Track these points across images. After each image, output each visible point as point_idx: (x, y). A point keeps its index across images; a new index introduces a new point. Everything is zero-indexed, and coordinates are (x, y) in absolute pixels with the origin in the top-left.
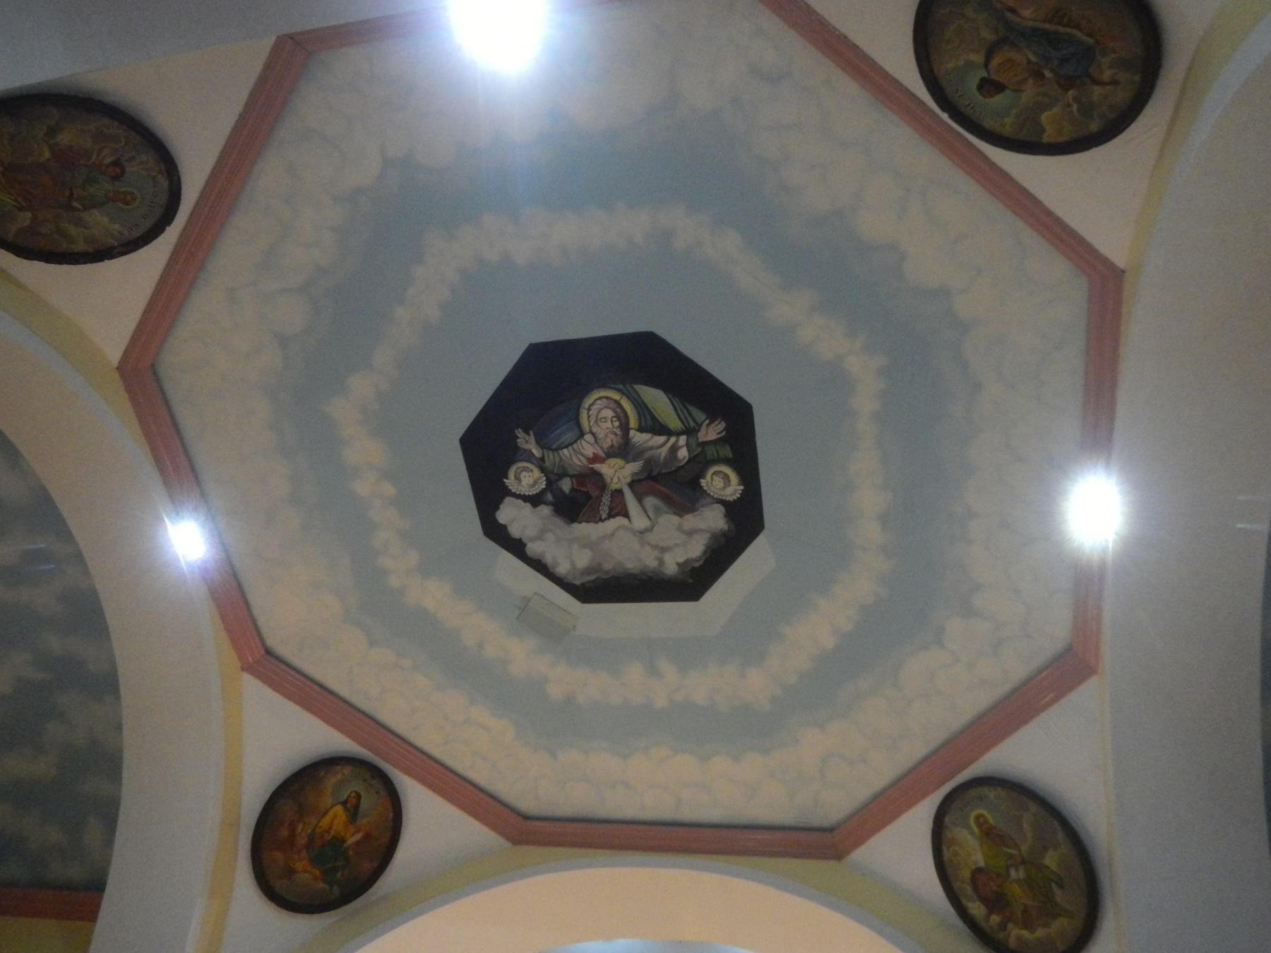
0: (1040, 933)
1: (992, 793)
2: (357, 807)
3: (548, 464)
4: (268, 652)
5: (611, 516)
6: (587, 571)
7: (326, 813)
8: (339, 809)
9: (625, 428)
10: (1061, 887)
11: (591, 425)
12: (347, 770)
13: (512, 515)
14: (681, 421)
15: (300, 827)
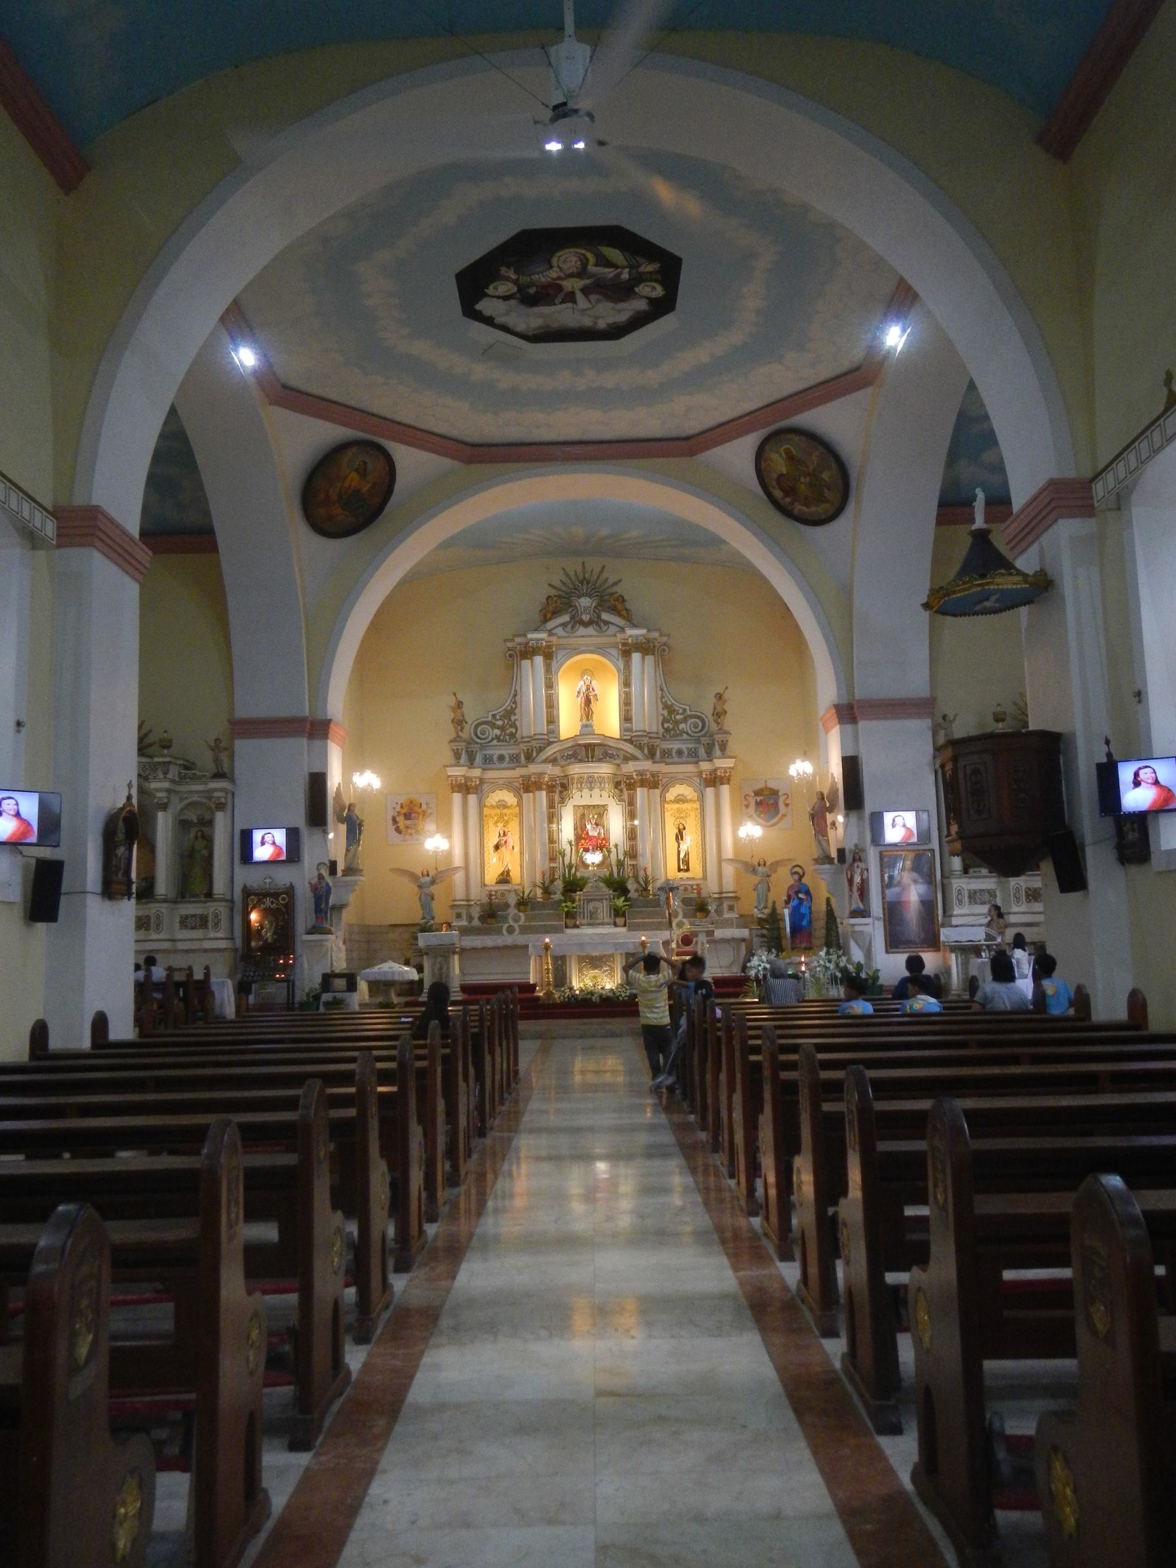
0: (813, 509)
1: (796, 438)
2: (365, 470)
3: (521, 281)
4: (284, 387)
5: (563, 302)
6: (539, 328)
7: (346, 478)
8: (354, 475)
9: (585, 263)
10: (829, 489)
11: (560, 262)
12: (354, 449)
13: (485, 306)
14: (627, 260)
15: (332, 490)
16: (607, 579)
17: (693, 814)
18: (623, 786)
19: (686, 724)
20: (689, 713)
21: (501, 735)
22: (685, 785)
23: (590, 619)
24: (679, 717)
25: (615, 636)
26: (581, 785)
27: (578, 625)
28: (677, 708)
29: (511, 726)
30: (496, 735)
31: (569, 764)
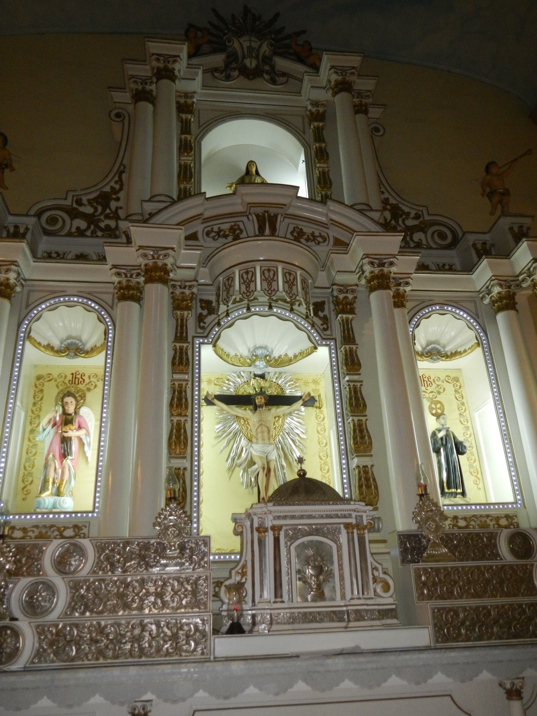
16: (283, 29)
17: (450, 388)
18: (329, 310)
19: (425, 233)
20: (427, 218)
21: (88, 228)
22: (448, 317)
23: (257, 67)
24: (410, 222)
25: (299, 93)
26: (248, 286)
27: (236, 73)
28: (406, 210)
29: (107, 217)
30: (78, 229)
31: (224, 247)
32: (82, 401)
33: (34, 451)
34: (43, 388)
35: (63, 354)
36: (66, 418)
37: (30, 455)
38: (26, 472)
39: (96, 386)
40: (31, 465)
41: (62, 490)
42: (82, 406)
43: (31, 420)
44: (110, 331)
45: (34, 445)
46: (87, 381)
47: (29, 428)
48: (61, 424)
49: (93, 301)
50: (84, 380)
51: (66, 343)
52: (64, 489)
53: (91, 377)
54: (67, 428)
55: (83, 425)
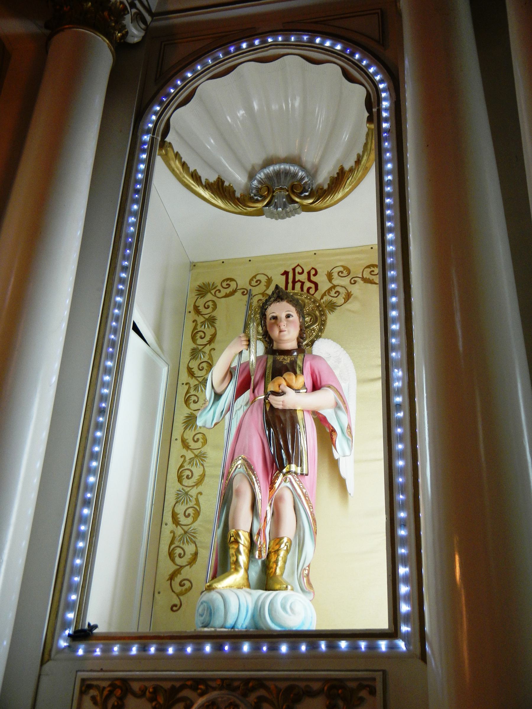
32: (316, 327)
33: (197, 471)
34: (214, 314)
35: (259, 205)
36: (274, 361)
37: (186, 482)
38: (179, 531)
39: (348, 296)
40: (190, 511)
41: (278, 572)
42: (318, 337)
43: (187, 392)
44: (384, 95)
45: (196, 456)
46: (324, 286)
47: (182, 412)
48: (264, 375)
49: (326, 35)
50: (316, 285)
51: (261, 175)
52: (283, 568)
53: (335, 275)
54: (281, 382)
55: (325, 379)
